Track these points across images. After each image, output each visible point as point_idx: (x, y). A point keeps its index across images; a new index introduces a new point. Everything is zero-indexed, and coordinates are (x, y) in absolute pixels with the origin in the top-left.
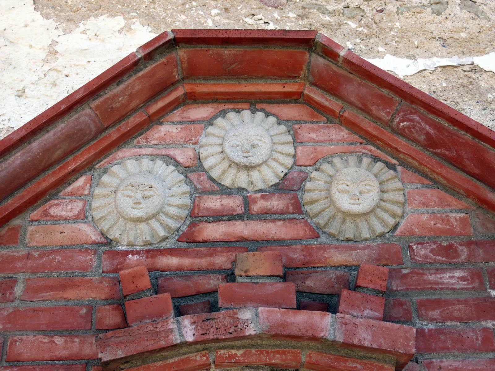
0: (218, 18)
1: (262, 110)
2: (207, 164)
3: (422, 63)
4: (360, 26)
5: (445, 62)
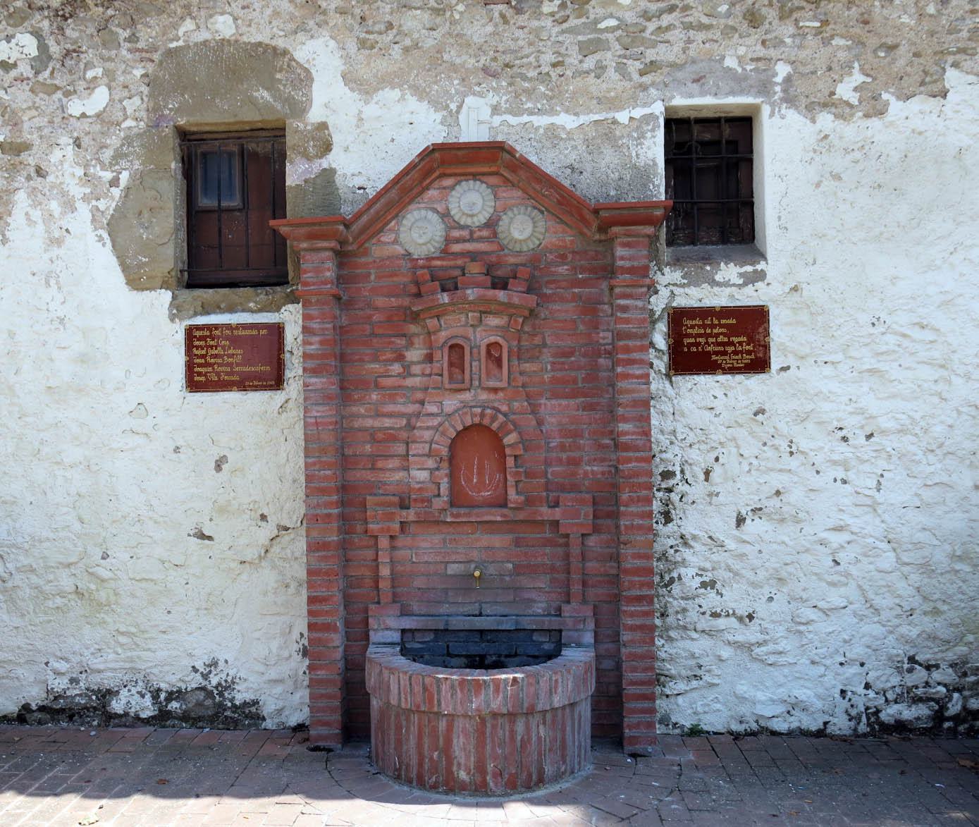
0: (458, 87)
1: (479, 180)
2: (452, 213)
3: (583, 119)
4: (548, 90)
5: (597, 117)
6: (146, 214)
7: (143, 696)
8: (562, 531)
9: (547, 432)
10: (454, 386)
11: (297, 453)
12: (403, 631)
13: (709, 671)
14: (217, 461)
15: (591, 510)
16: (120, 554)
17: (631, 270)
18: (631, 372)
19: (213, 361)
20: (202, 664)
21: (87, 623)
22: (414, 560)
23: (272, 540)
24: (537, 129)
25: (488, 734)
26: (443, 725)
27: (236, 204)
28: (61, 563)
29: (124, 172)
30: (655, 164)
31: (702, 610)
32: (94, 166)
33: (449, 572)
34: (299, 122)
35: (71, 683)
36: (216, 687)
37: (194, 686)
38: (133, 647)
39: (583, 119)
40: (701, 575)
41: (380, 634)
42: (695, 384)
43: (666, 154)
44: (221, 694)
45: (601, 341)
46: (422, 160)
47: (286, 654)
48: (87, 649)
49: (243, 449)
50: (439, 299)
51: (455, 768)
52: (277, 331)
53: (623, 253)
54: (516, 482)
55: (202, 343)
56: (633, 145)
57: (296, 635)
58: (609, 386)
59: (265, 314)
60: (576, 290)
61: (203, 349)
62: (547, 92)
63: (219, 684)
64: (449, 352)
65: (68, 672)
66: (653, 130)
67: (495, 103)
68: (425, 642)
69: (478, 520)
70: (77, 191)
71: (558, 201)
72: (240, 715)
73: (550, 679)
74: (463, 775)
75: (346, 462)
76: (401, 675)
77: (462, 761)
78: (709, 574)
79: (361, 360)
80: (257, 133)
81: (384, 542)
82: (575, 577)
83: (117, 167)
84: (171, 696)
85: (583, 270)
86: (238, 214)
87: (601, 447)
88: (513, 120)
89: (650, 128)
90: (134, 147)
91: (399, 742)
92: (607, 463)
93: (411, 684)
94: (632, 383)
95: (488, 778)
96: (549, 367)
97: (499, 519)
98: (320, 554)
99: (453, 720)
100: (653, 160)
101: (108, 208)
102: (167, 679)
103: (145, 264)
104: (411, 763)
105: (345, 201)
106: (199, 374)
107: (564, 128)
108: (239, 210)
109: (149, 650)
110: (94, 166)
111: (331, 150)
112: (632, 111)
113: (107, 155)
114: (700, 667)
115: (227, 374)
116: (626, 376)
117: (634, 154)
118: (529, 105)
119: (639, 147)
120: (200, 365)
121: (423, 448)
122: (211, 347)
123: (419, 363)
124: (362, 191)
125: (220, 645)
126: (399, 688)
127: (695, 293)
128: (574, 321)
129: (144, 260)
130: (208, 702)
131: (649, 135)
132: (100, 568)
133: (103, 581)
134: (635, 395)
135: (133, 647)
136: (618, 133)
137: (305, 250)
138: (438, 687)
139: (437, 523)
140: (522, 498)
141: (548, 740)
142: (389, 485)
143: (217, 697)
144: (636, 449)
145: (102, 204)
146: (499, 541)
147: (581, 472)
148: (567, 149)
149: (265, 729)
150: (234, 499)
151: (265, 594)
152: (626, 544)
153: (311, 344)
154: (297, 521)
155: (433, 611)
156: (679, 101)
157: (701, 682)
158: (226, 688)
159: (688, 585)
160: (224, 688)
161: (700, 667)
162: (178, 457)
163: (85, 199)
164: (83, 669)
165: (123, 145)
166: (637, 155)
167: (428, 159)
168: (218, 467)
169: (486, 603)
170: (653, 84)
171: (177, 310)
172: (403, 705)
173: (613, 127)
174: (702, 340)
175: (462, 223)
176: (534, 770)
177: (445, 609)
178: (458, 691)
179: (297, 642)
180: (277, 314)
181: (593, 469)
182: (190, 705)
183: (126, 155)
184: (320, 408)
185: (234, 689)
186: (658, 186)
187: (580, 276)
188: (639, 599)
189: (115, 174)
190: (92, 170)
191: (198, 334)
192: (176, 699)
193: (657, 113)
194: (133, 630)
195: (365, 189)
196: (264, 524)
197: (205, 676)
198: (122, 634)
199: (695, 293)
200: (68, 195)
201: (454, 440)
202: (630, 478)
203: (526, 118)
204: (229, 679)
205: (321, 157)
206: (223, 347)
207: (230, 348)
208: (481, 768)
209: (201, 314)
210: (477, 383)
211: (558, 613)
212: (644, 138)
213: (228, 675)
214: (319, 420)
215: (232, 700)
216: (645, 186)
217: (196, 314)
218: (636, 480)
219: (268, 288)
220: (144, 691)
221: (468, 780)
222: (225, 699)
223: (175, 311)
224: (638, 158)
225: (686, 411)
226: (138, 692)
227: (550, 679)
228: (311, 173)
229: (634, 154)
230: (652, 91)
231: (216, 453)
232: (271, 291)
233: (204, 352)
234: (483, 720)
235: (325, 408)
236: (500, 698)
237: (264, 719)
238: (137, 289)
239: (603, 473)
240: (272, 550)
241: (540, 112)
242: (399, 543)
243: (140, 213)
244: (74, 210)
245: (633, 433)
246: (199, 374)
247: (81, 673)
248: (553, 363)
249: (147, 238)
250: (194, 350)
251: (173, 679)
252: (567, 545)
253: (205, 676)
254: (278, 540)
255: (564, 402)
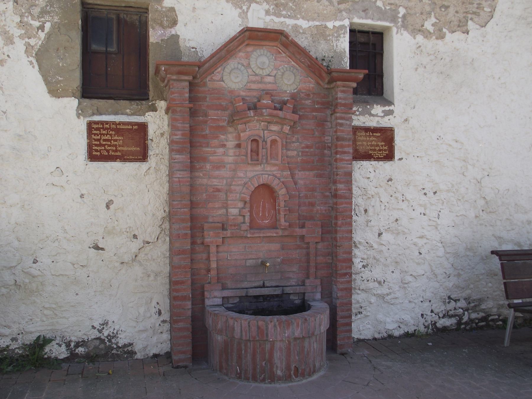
3: (311, 23)
4: (293, 5)
6: (62, 51)
7: (60, 346)
8: (306, 241)
9: (298, 188)
10: (253, 162)
11: (155, 198)
12: (223, 298)
13: (365, 309)
14: (107, 203)
15: (320, 230)
16: (45, 260)
17: (344, 105)
18: (343, 158)
19: (104, 143)
20: (98, 324)
21: (23, 303)
22: (229, 258)
23: (139, 249)
24: (289, 25)
25: (292, 349)
26: (268, 347)
27: (114, 50)
28: (5, 267)
29: (47, 22)
30: (345, 52)
31: (363, 279)
32: (27, 17)
33: (248, 264)
34: (158, 5)
35: (12, 341)
36: (107, 337)
37: (93, 337)
38: (54, 316)
39: (311, 23)
40: (362, 262)
41: (211, 300)
42: (362, 165)
43: (350, 47)
44: (110, 341)
45: (326, 141)
46: (240, 35)
47: (149, 315)
48: (23, 319)
49: (122, 196)
50: (248, 114)
51: (275, 369)
52: (143, 127)
53: (341, 96)
54: (285, 215)
55: (98, 132)
56: (335, 40)
57: (154, 303)
58: (329, 165)
59: (136, 117)
60: (314, 114)
61: (98, 135)
62: (293, 7)
63: (109, 335)
64: (251, 144)
65: (10, 334)
66: (344, 34)
67: (267, 9)
68: (234, 303)
69: (265, 235)
70: (17, 32)
71: (308, 65)
72: (121, 352)
73: (320, 318)
74: (279, 373)
75: (193, 205)
76: (243, 321)
77: (279, 365)
78: (365, 261)
79: (201, 146)
80: (127, 9)
81: (213, 249)
82: (312, 264)
83: (42, 19)
84: (77, 345)
85: (318, 103)
86: (114, 56)
87: (326, 197)
88: (276, 19)
89: (343, 32)
90: (54, 8)
91: (240, 357)
92: (327, 205)
93: (249, 326)
94: (344, 164)
95: (292, 373)
96: (300, 154)
97: (275, 235)
98: (180, 256)
99: (274, 344)
100: (344, 49)
101: (36, 44)
102: (76, 335)
103: (60, 81)
104: (248, 369)
105: (184, 54)
106: (97, 151)
107: (301, 27)
108: (115, 54)
109: (64, 317)
110: (27, 17)
111: (177, 24)
112: (335, 22)
113: (36, 11)
114: (361, 307)
115: (113, 151)
116: (342, 160)
117: (335, 45)
118: (284, 13)
119: (337, 41)
120: (96, 145)
121: (236, 196)
122: (104, 134)
123: (232, 149)
124: (194, 50)
125: (109, 312)
126: (241, 329)
127: (362, 119)
128: (313, 130)
129: (60, 78)
130: (102, 346)
131: (342, 36)
132: (32, 269)
133: (34, 277)
134: (345, 170)
135: (54, 316)
136: (327, 33)
137: (174, 80)
138: (267, 326)
139: (241, 237)
140: (288, 224)
141: (317, 350)
142: (215, 217)
143: (108, 343)
144: (345, 198)
145: (32, 42)
146: (275, 246)
147: (315, 209)
148: (302, 38)
149: (137, 359)
150: (117, 226)
151: (136, 280)
152: (339, 247)
153: (176, 135)
154: (155, 238)
155: (239, 286)
156: (356, 20)
157: (362, 315)
158: (113, 337)
159: (356, 267)
160: (110, 338)
161: (361, 307)
162: (83, 201)
163: (21, 37)
164: (20, 332)
165: (47, 6)
166: (337, 45)
167: (242, 35)
168: (108, 207)
169: (267, 280)
170: (344, 10)
171: (82, 111)
172: (244, 338)
173: (325, 30)
174: (365, 143)
175: (257, 73)
176: (311, 366)
177: (245, 285)
178: (278, 328)
179: (155, 308)
180: (143, 117)
181: (320, 208)
182: (90, 349)
183: (49, 13)
184: (182, 173)
185: (118, 337)
186: (346, 63)
187: (316, 106)
188: (345, 274)
189: (41, 23)
190: (26, 19)
191: (95, 126)
192: (82, 346)
193: (346, 25)
194: (54, 306)
195: (196, 49)
196: (135, 240)
197: (100, 331)
198: (46, 308)
199: (362, 119)
200: (9, 33)
201: (253, 192)
202: (342, 213)
203: (282, 19)
204: (115, 332)
205: (171, 28)
206: (111, 135)
207: (115, 135)
208: (288, 368)
209: (97, 115)
210: (265, 161)
211: (303, 284)
212: (340, 37)
213: (114, 329)
214: (180, 179)
215: (117, 344)
216: (340, 62)
217: (93, 114)
218: (345, 214)
219: (138, 102)
220: (61, 343)
221: (282, 375)
222: (112, 343)
223: (80, 112)
224: (337, 47)
225: (358, 179)
226: (57, 344)
227: (320, 318)
228: (165, 36)
229: (335, 45)
230: (344, 13)
231: (107, 198)
232: (140, 103)
233: (99, 137)
234: (289, 342)
235: (184, 173)
236: (299, 329)
237: (136, 353)
238: (56, 97)
239: (325, 210)
240: (139, 255)
241: (289, 17)
242: (221, 249)
243: (58, 50)
244: (12, 43)
245: (344, 190)
246: (97, 151)
247: (19, 334)
248: (302, 152)
249: (63, 66)
250: (93, 136)
251: (80, 334)
252: (308, 248)
253: (100, 331)
254: (143, 249)
255: (307, 173)
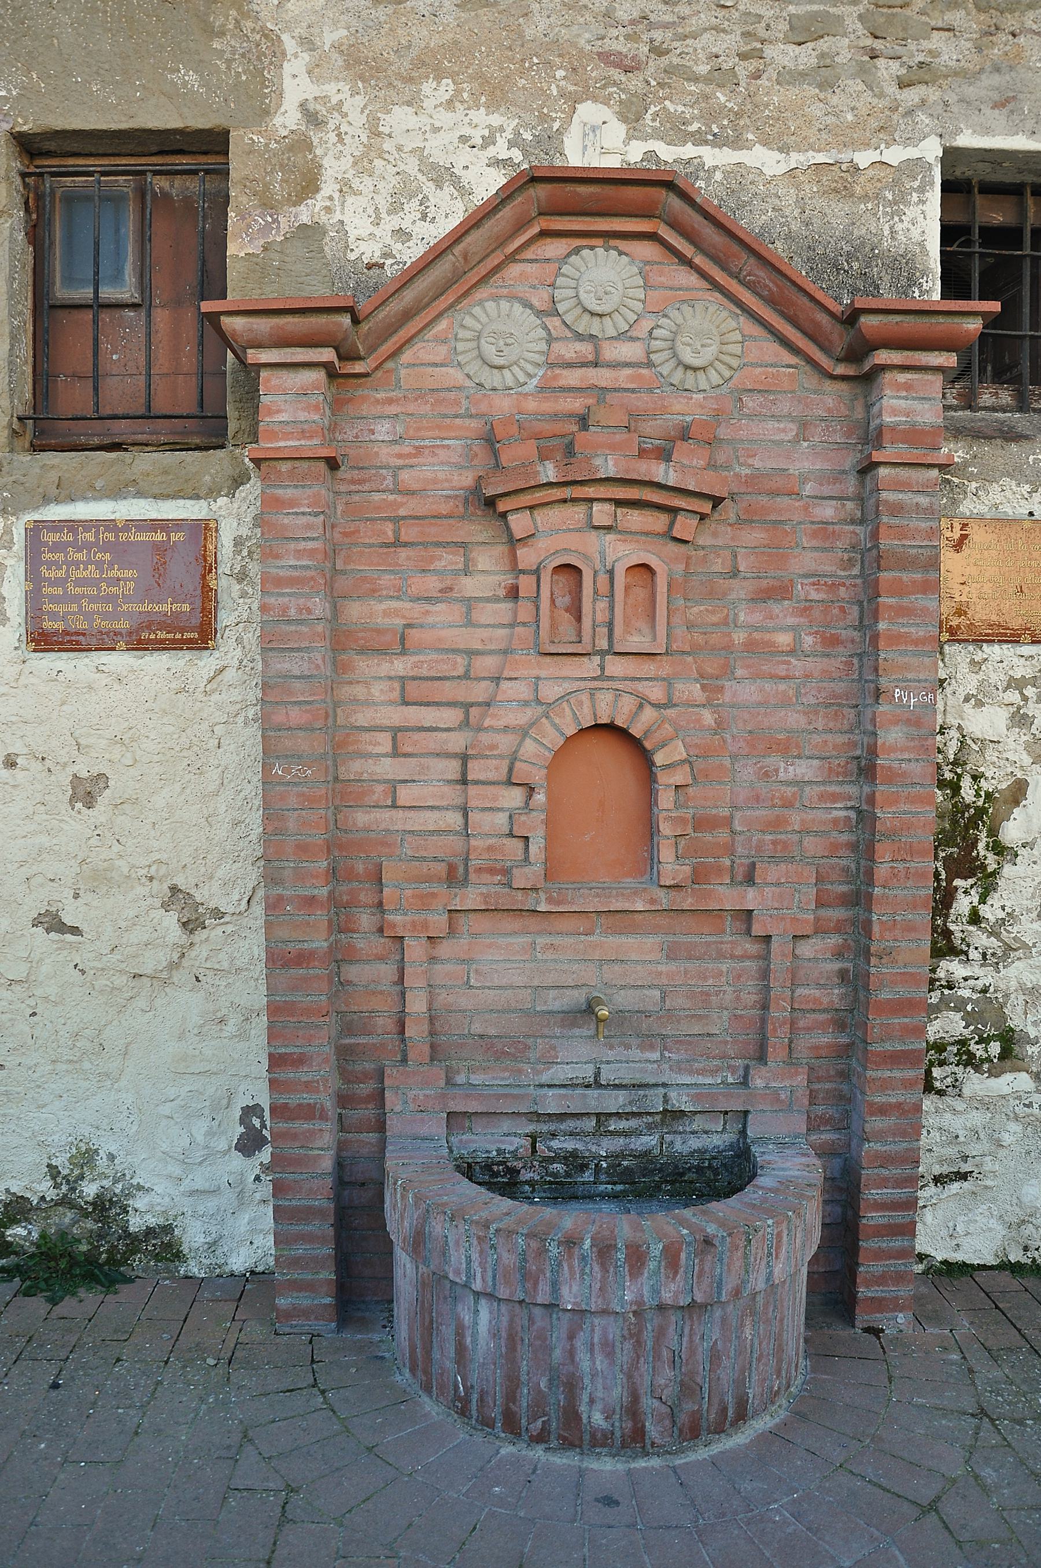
0: (563, 83)
1: (616, 248)
2: (561, 308)
3: (796, 159)
5: (821, 158)
39: (796, 159)
50: (538, 472)
55: (59, 556)
56: (886, 213)
59: (181, 502)
66: (921, 190)
81: (415, 949)
82: (779, 1013)
100: (922, 244)
108: (134, 306)
115: (105, 615)
119: (896, 219)
120: (55, 599)
122: (77, 564)
149: (187, 1277)
156: (967, 140)
161: (965, 1158)
166: (893, 232)
193: (931, 159)
206: (99, 564)
207: (111, 564)
209: (57, 501)
217: (47, 500)
230: (922, 117)
233: (61, 574)
252: (766, 957)
